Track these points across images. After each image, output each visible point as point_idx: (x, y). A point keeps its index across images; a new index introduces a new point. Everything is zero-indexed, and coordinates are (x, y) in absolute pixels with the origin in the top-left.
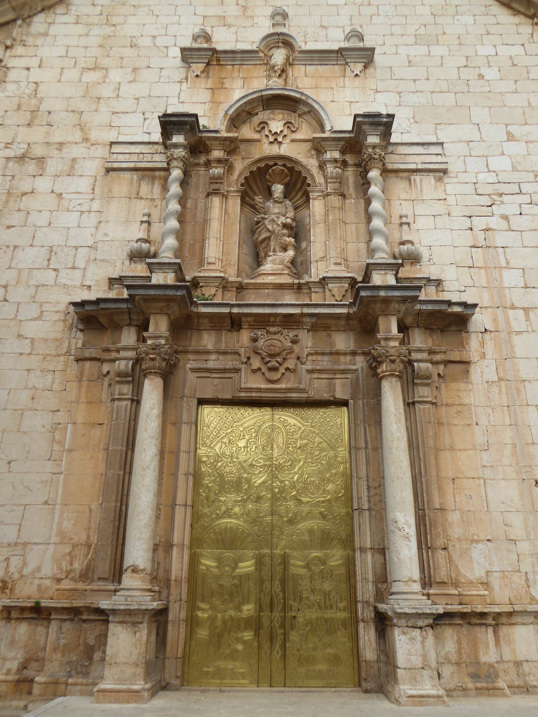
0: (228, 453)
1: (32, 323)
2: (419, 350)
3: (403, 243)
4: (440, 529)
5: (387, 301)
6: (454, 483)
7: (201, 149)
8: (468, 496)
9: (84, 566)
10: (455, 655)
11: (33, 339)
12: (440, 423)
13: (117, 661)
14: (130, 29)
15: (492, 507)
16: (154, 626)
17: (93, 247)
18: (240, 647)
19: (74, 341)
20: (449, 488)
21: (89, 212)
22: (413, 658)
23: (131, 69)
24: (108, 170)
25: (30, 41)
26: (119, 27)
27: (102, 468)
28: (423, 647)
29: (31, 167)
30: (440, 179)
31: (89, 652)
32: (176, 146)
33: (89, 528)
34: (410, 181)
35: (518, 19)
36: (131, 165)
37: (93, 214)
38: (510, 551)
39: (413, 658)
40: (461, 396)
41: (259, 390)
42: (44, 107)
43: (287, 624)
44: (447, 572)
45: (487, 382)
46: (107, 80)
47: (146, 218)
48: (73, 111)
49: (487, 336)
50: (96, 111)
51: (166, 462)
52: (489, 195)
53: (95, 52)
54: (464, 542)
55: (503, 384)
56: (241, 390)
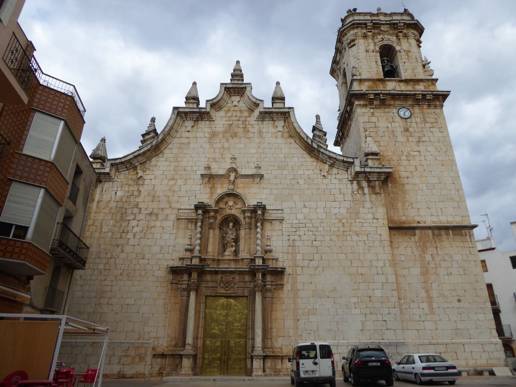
2: (268, 281)
3: (267, 246)
4: (270, 334)
5: (258, 269)
17: (174, 246)
18: (216, 365)
24: (178, 219)
25: (151, 168)
27: (179, 316)
29: (154, 217)
30: (281, 222)
31: (177, 366)
32: (199, 214)
35: (312, 159)
36: (185, 218)
41: (223, 293)
42: (157, 195)
43: (228, 359)
47: (190, 237)
49: (290, 276)
53: (173, 172)
56: (218, 293)
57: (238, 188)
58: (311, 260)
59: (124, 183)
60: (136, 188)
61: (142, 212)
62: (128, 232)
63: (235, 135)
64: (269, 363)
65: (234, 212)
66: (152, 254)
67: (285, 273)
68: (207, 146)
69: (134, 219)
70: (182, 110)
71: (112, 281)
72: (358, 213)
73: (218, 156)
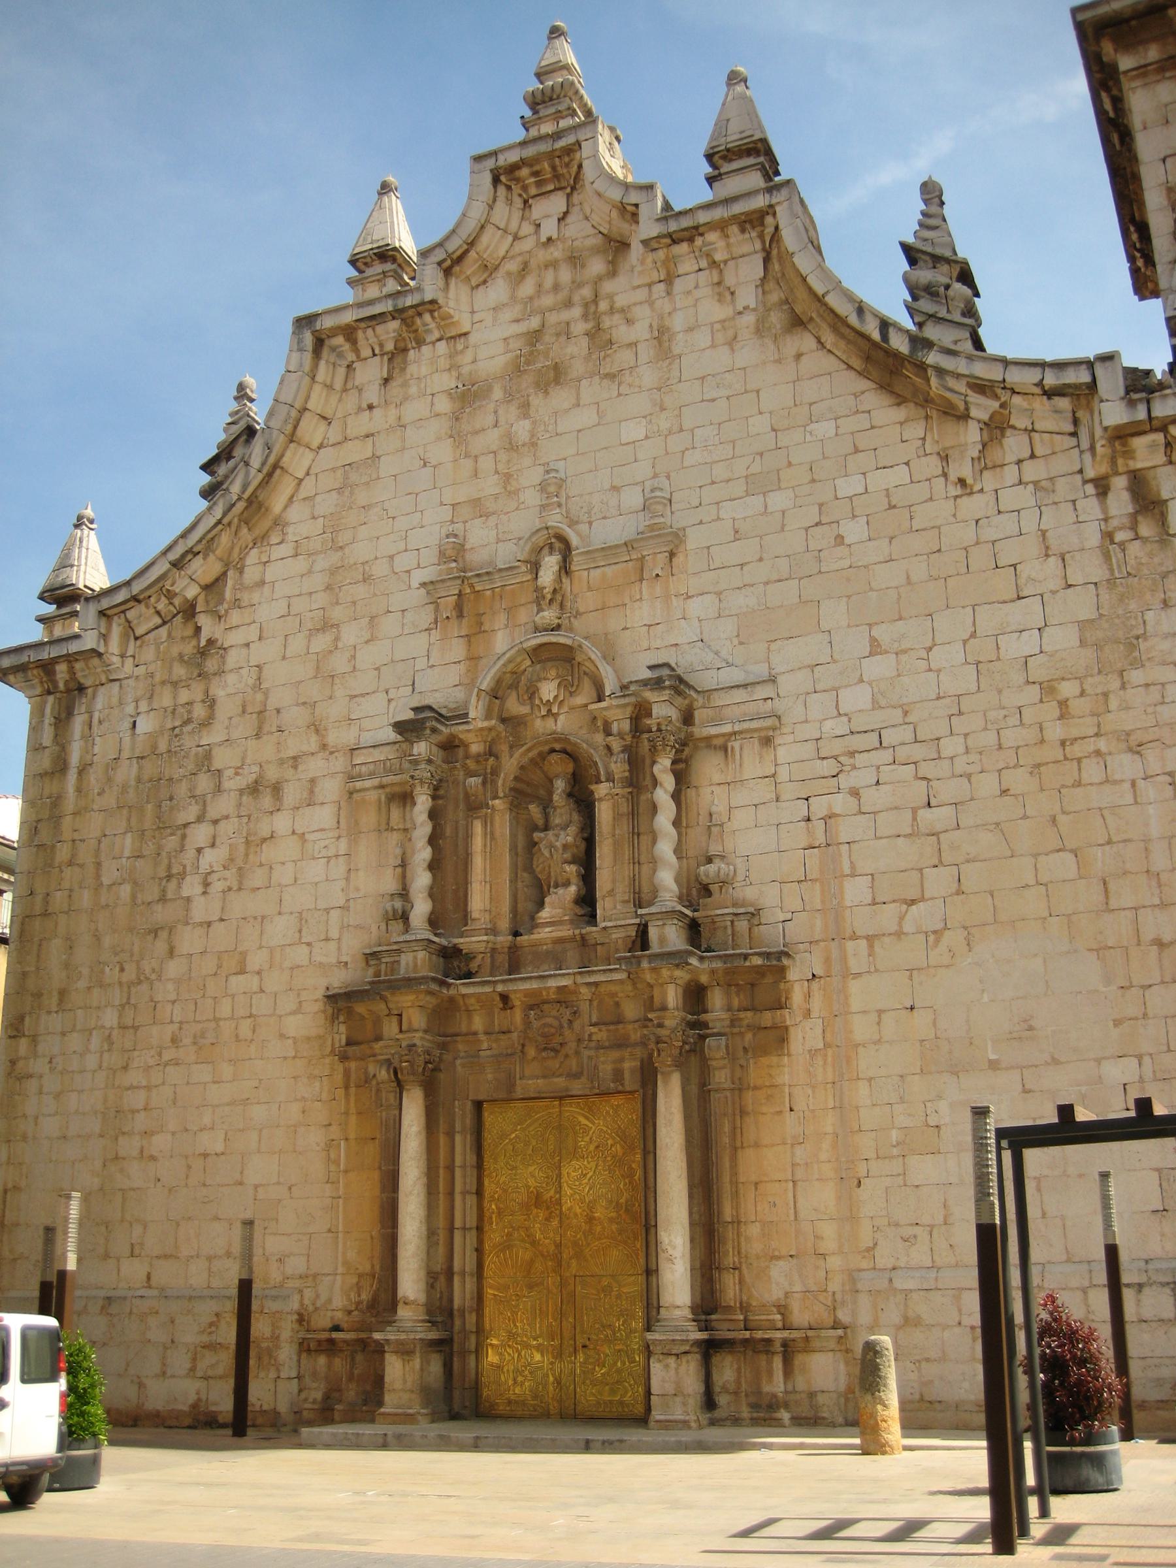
1: (291, 1018)
3: (709, 860)
6: (756, 1189)
7: (457, 742)
11: (294, 1038)
12: (743, 1113)
14: (361, 551)
15: (802, 1214)
17: (345, 908)
19: (337, 1037)
21: (337, 856)
22: (666, 1385)
23: (367, 619)
25: (245, 597)
26: (347, 550)
27: (377, 1192)
28: (677, 1373)
29: (267, 801)
30: (767, 741)
34: (726, 751)
35: (900, 413)
37: (341, 859)
38: (817, 1268)
39: (666, 1385)
42: (272, 704)
45: (810, 1051)
46: (340, 645)
48: (304, 703)
49: (815, 985)
50: (331, 698)
52: (835, 758)
53: (321, 599)
55: (830, 1052)
57: (578, 614)
58: (913, 902)
59: (158, 678)
60: (195, 692)
61: (227, 784)
62: (183, 875)
63: (556, 375)
64: (727, 1370)
65: (563, 724)
66: (272, 950)
67: (793, 975)
68: (443, 452)
69: (200, 819)
70: (328, 323)
71: (148, 1068)
72: (1132, 644)
73: (490, 485)
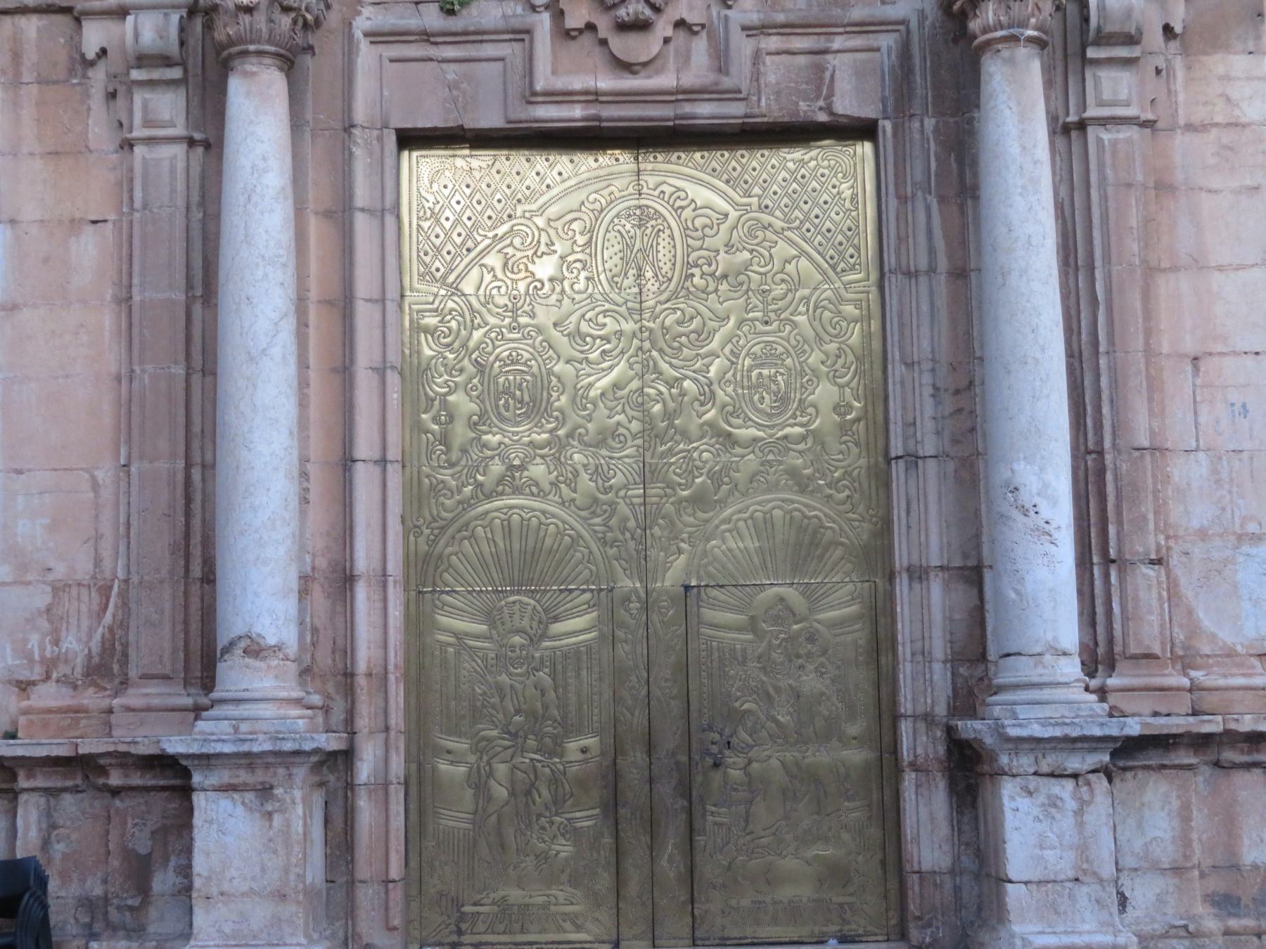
0: (502, 301)
4: (1148, 508)
6: (1196, 369)
8: (1237, 408)
9: (95, 644)
10: (1170, 848)
12: (1164, 187)
13: (226, 887)
16: (318, 799)
20: (1179, 383)
28: (1081, 825)
31: (140, 872)
33: (98, 538)
40: (1235, 94)
41: (593, 96)
44: (1162, 626)
51: (312, 331)
54: (1217, 542)
